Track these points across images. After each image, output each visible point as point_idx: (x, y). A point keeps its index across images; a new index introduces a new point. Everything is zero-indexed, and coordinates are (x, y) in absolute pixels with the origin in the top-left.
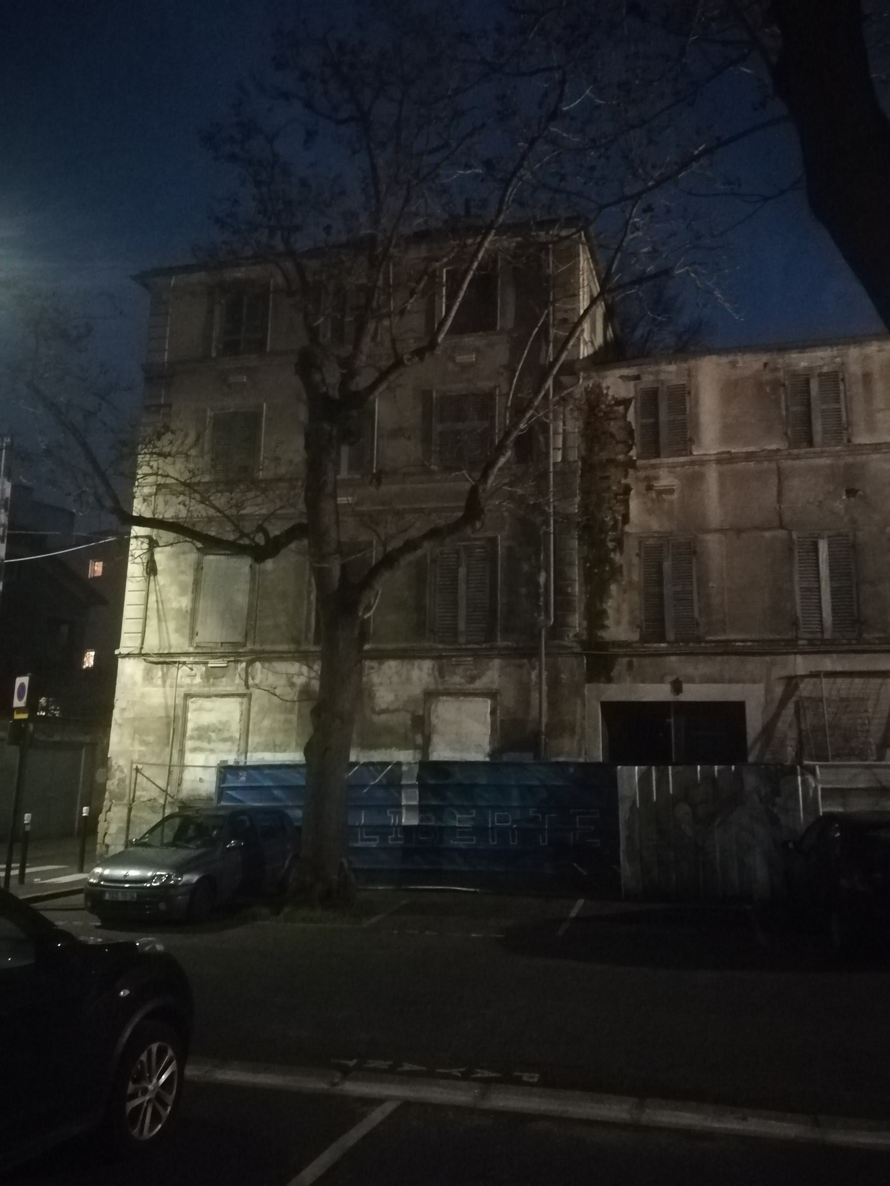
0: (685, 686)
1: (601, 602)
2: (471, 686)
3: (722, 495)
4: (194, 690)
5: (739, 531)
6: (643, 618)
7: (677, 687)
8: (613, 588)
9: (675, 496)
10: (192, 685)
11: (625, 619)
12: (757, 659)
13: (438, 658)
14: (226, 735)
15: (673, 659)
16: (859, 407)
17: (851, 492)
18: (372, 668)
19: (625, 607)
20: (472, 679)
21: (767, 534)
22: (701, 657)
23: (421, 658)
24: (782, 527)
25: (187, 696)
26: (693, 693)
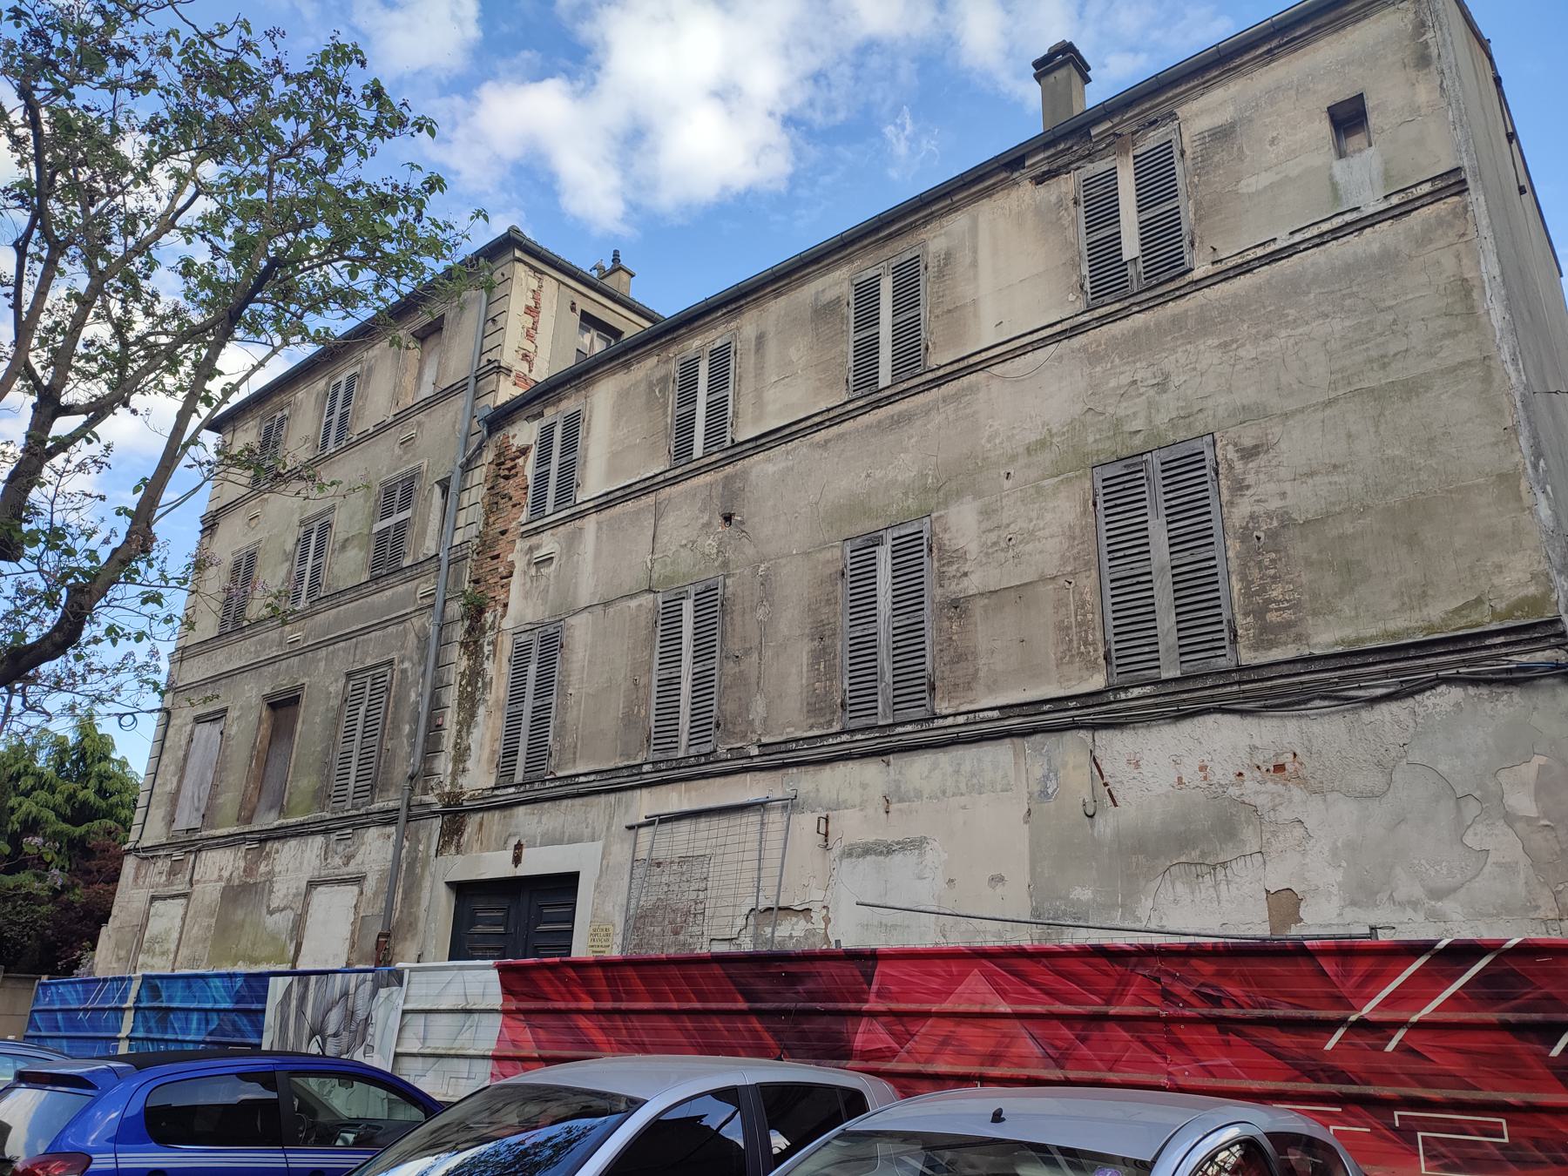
0: (526, 853)
1: (469, 733)
2: (345, 870)
3: (598, 555)
4: (162, 891)
5: (606, 604)
6: (501, 752)
7: (517, 860)
8: (481, 711)
9: (553, 567)
10: (158, 885)
11: (486, 754)
12: (603, 799)
13: (326, 832)
14: (166, 947)
15: (521, 810)
16: (748, 386)
17: (728, 518)
18: (277, 852)
19: (488, 736)
20: (349, 859)
21: (633, 603)
22: (547, 805)
23: (313, 833)
24: (650, 590)
25: (154, 898)
26: (538, 862)
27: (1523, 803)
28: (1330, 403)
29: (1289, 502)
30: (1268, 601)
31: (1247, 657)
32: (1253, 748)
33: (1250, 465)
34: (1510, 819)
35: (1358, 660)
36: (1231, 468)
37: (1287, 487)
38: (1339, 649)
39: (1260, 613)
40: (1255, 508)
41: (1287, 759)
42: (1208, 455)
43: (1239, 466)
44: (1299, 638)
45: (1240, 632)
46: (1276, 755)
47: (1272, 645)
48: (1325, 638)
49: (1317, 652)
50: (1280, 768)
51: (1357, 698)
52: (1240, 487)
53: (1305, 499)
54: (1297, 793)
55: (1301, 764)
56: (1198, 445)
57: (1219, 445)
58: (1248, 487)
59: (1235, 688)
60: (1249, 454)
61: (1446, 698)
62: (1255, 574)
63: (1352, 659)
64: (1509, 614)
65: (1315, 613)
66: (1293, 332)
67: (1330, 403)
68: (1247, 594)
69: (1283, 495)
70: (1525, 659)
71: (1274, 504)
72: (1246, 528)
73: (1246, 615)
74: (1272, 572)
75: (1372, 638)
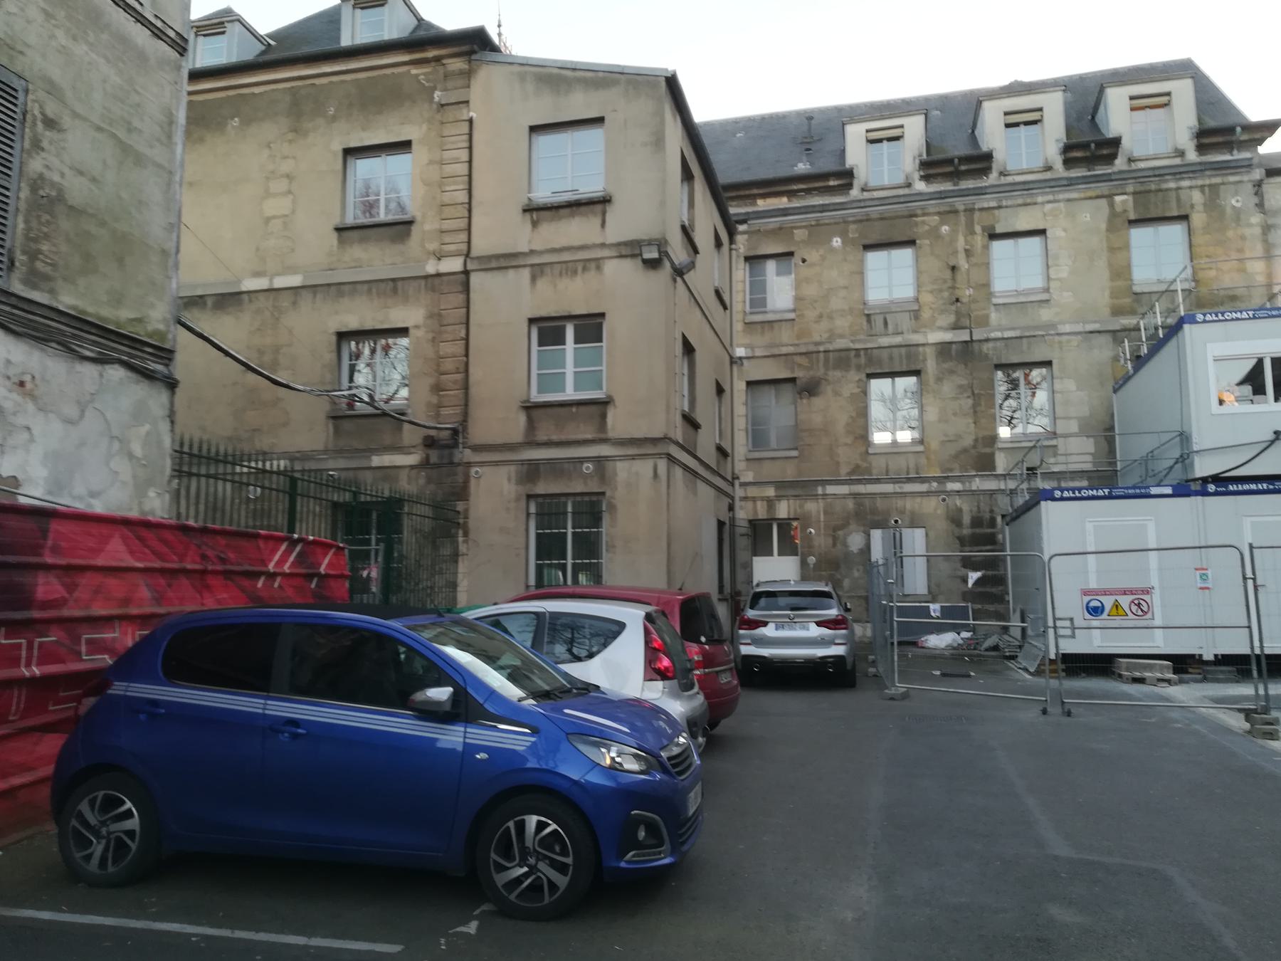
27: (137, 450)
28: (99, 129)
29: (65, 183)
30: (40, 252)
31: (18, 288)
32: (8, 362)
33: (47, 133)
34: (131, 456)
35: (86, 328)
36: (34, 124)
37: (66, 171)
38: (73, 313)
39: (33, 256)
40: (44, 171)
41: (27, 378)
42: (21, 95)
43: (40, 126)
44: (52, 292)
45: (17, 264)
46: (23, 373)
47: (34, 287)
48: (67, 300)
49: (61, 308)
50: (22, 384)
51: (77, 352)
52: (37, 146)
53: (77, 189)
54: (30, 407)
55: (36, 386)
56: (16, 83)
57: (30, 97)
58: (43, 149)
59: (7, 309)
60: (50, 123)
61: (116, 373)
62: (34, 224)
63: (81, 323)
64: (150, 336)
65: (65, 279)
66: (89, 52)
67: (99, 129)
68: (27, 238)
69: (63, 175)
70: (153, 364)
71: (56, 178)
72: (35, 181)
73: (24, 252)
74: (45, 230)
75: (90, 315)
